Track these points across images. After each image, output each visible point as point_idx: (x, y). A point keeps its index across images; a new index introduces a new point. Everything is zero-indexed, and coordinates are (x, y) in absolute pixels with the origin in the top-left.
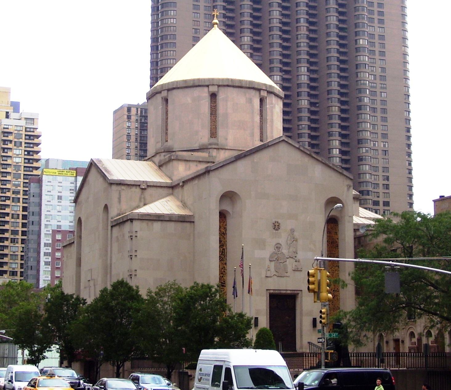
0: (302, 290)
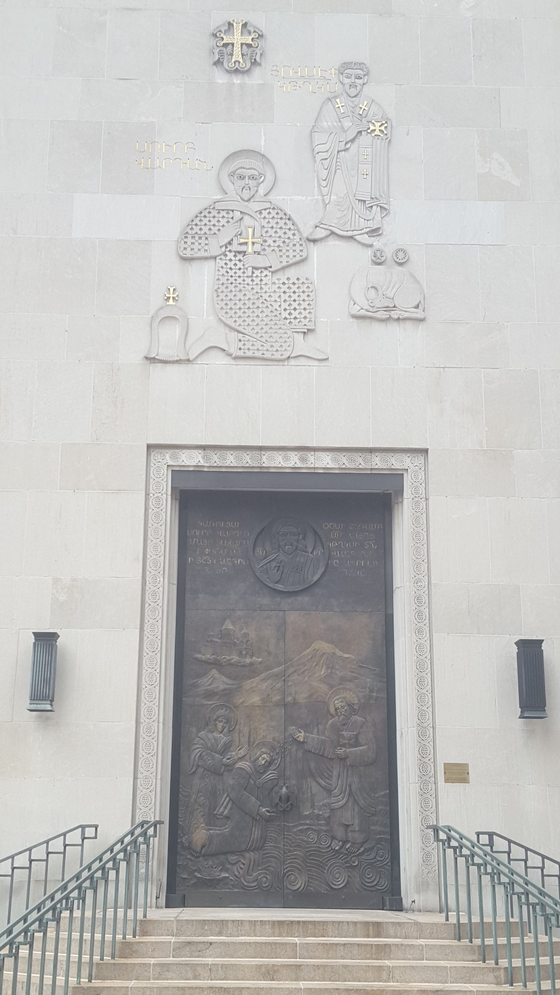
0: (426, 451)
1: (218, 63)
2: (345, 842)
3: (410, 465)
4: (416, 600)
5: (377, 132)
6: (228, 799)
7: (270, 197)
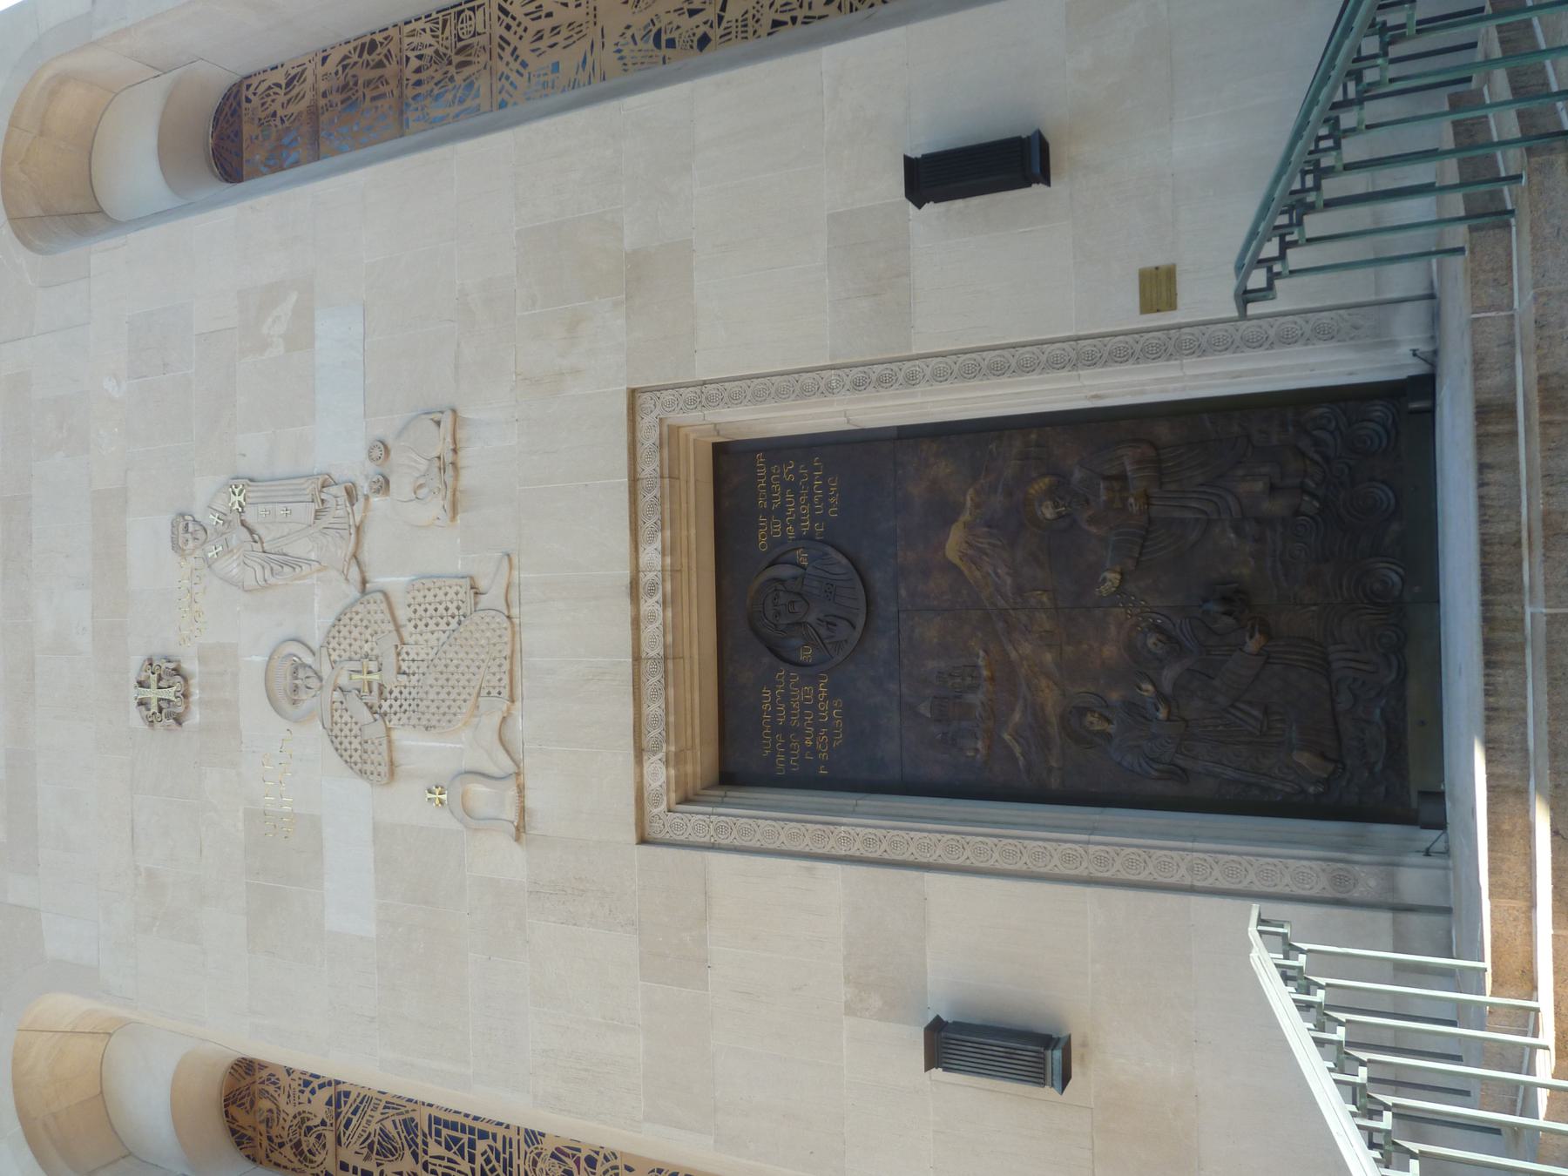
0: (633, 394)
1: (178, 720)
2: (1303, 489)
3: (654, 415)
4: (860, 388)
5: (241, 498)
6: (1233, 711)
7: (315, 645)
